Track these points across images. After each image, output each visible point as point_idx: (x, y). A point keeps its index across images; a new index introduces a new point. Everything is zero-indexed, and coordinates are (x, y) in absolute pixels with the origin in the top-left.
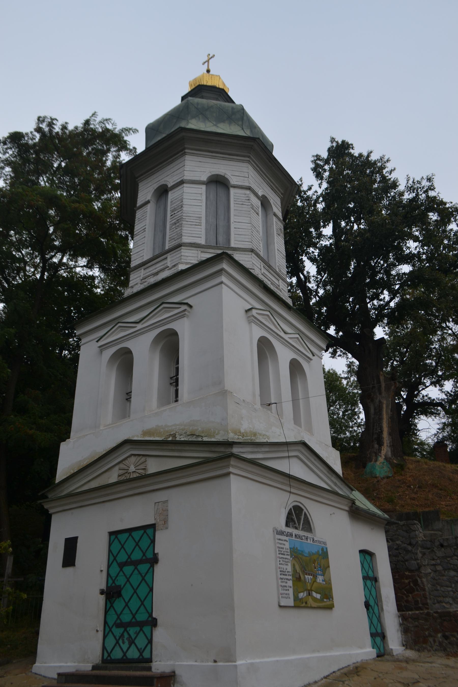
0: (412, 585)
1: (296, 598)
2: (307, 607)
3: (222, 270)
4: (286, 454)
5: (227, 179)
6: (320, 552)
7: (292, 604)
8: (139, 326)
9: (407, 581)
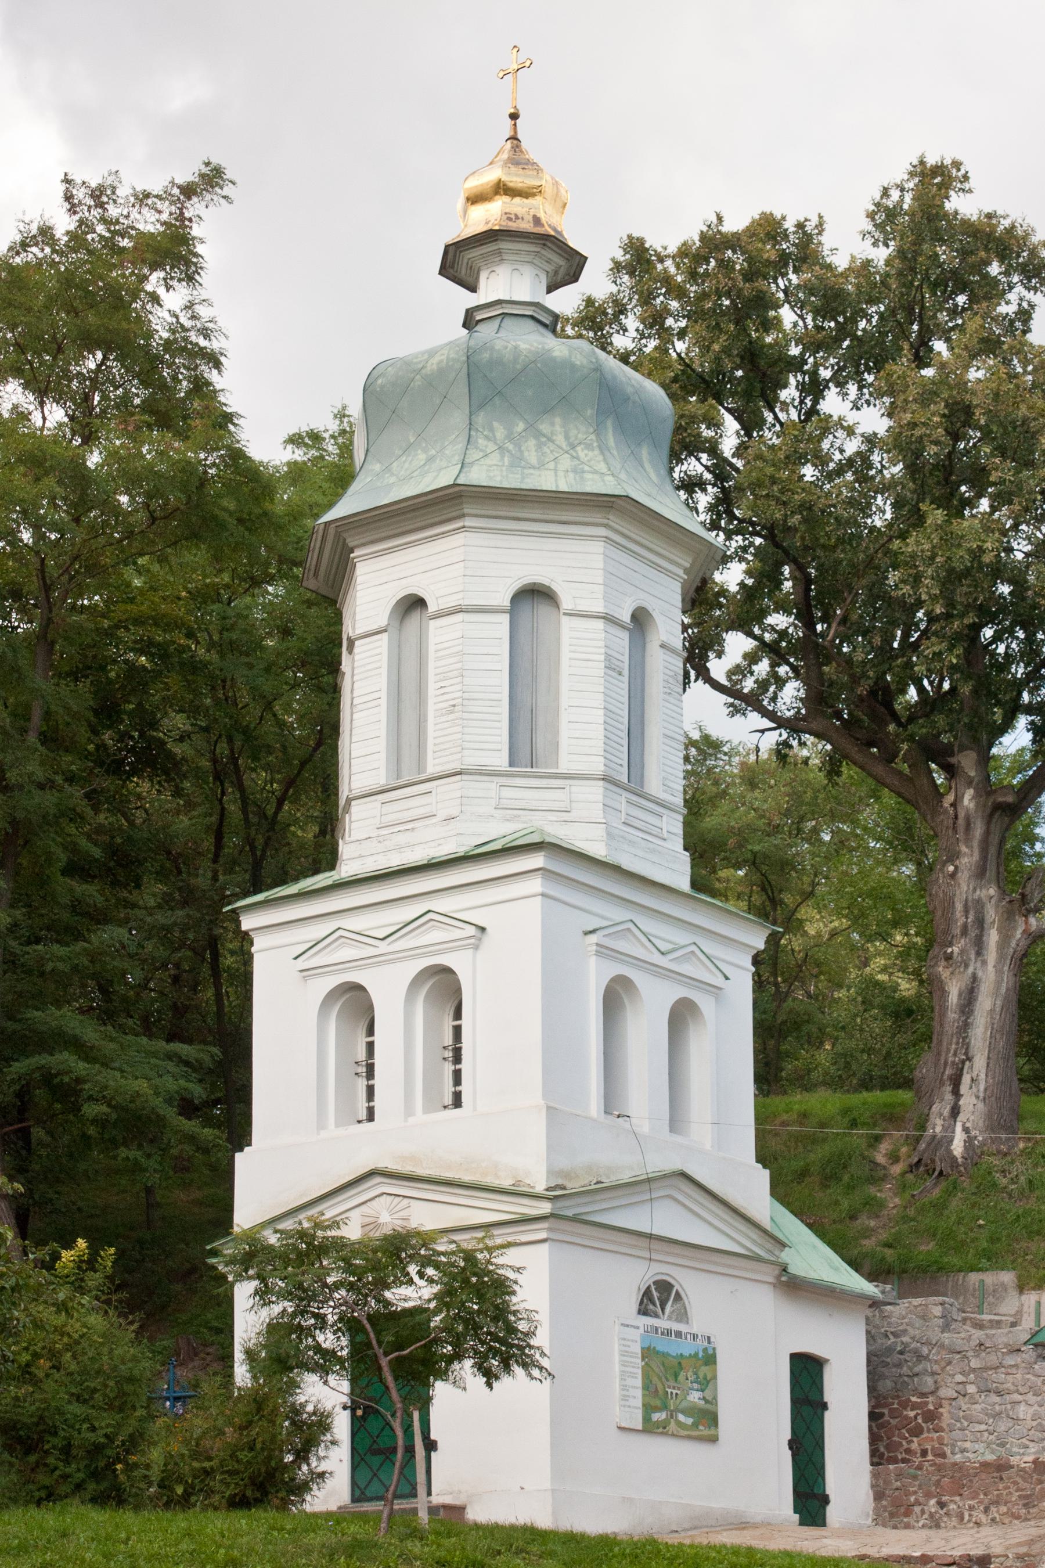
0: (920, 1421)
1: (647, 1419)
2: (665, 1434)
6: (701, 1354)
7: (640, 1427)
8: (383, 947)
9: (912, 1414)
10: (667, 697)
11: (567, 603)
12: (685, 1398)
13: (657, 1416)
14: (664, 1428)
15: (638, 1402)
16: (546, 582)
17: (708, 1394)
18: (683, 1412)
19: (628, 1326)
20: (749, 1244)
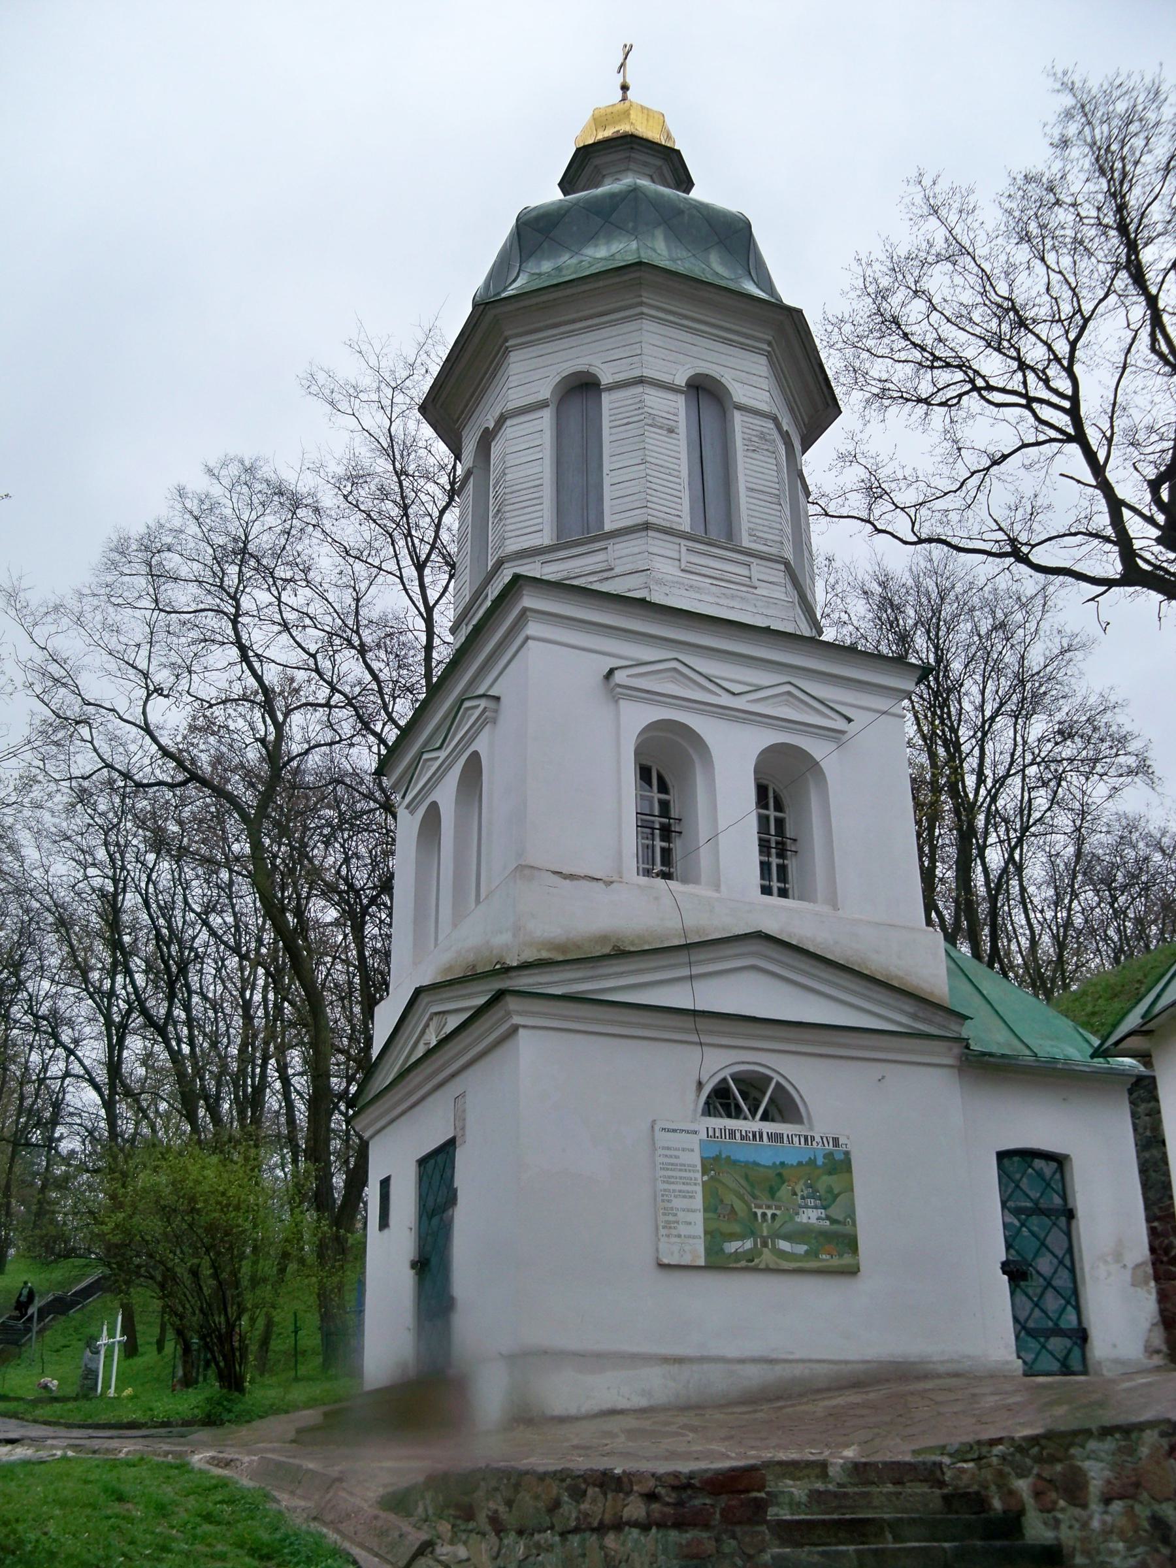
2: (756, 1269)
3: (525, 610)
4: (685, 972)
5: (594, 376)
6: (820, 1161)
8: (443, 754)
10: (750, 454)
11: (605, 379)
12: (792, 1219)
13: (732, 1247)
14: (752, 1261)
15: (699, 1229)
16: (584, 368)
17: (836, 1211)
18: (787, 1238)
19: (674, 1131)
20: (904, 1019)
